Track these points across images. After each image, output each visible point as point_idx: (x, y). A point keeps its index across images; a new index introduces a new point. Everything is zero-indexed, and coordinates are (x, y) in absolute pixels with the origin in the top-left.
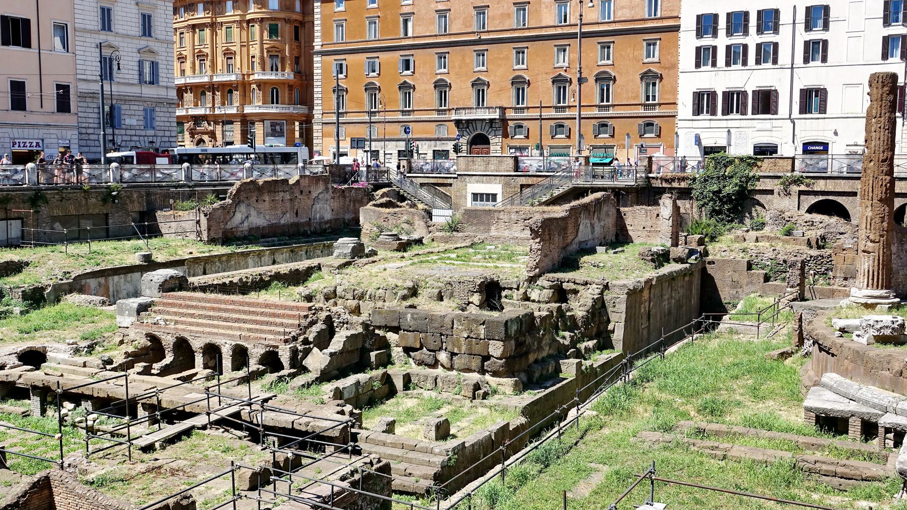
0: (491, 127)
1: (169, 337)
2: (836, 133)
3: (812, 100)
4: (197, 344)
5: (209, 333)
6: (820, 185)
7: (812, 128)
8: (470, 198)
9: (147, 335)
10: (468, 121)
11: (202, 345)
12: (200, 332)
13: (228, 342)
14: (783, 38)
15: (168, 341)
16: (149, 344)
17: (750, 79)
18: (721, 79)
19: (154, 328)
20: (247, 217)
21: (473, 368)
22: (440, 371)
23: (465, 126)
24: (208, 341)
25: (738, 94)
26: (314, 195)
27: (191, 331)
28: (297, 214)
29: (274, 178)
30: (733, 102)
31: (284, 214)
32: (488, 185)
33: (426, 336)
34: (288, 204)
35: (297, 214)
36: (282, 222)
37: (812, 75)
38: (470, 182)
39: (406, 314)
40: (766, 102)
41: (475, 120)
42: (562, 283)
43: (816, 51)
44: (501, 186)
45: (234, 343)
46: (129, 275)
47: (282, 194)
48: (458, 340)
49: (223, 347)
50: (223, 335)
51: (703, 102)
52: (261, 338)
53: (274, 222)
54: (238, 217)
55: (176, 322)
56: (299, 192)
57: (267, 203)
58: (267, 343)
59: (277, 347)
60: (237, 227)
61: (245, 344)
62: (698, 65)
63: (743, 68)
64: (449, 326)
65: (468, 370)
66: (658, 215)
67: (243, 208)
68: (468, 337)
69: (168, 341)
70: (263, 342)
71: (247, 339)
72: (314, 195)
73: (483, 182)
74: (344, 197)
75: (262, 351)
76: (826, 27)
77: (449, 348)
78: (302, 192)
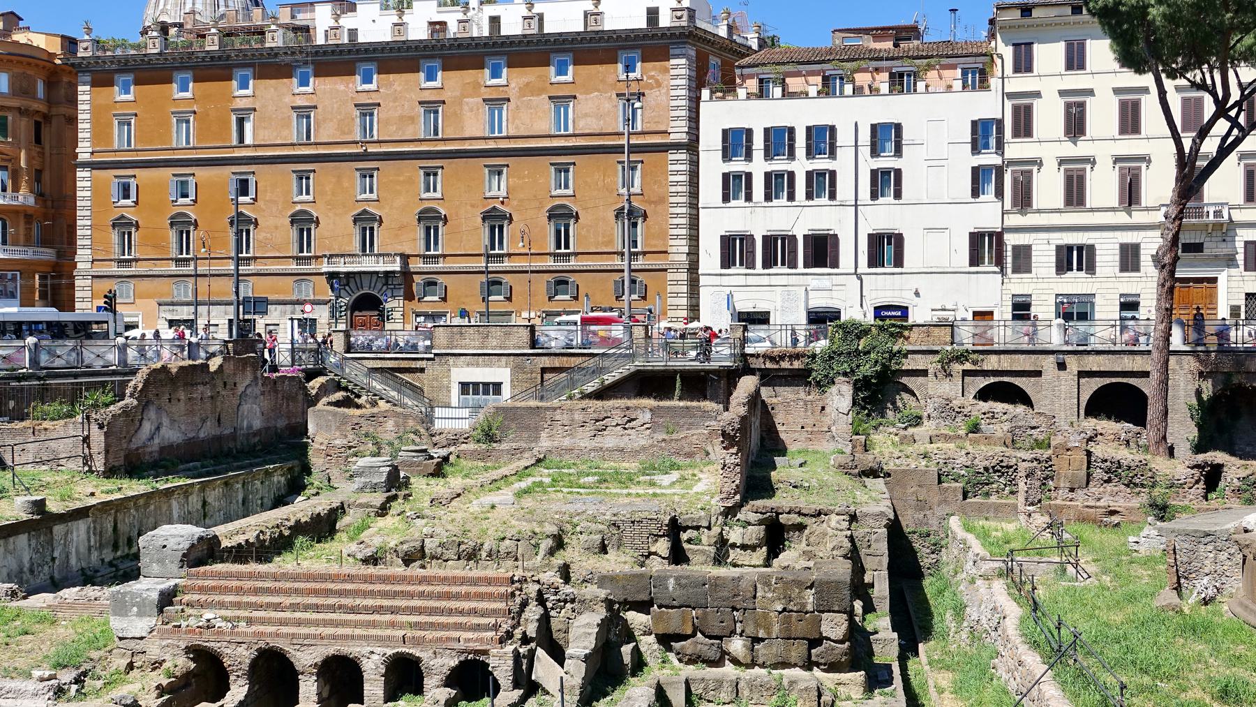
0: (386, 284)
1: (241, 650)
2: (917, 294)
3: (886, 249)
4: (305, 658)
5: (334, 637)
6: (992, 363)
7: (886, 287)
8: (455, 390)
9: (188, 650)
10: (348, 274)
11: (319, 660)
12: (315, 637)
13: (378, 650)
14: (842, 164)
15: (238, 657)
16: (193, 666)
18: (760, 219)
19: (207, 635)
20: (158, 428)
21: (793, 661)
22: (729, 669)
23: (344, 281)
24: (331, 651)
25: (783, 239)
26: (241, 389)
27: (293, 636)
28: (219, 420)
29: (191, 362)
30: (777, 250)
31: (204, 421)
32: (487, 370)
33: (705, 614)
34: (208, 405)
35: (219, 420)
36: (202, 435)
38: (456, 365)
39: (666, 578)
40: (822, 250)
41: (360, 273)
42: (778, 514)
43: (885, 183)
45: (390, 652)
46: (11, 540)
47: (201, 388)
48: (765, 616)
49: (365, 661)
50: (366, 638)
51: (734, 249)
52: (448, 639)
53: (191, 435)
54: (147, 427)
55: (250, 621)
56: (221, 384)
57: (182, 404)
58: (462, 645)
59: (485, 652)
60: (145, 446)
61: (416, 652)
62: (726, 198)
63: (747, 204)
64: (749, 595)
65: (785, 665)
66: (823, 408)
67: (152, 413)
68: (784, 610)
69: (238, 657)
70: (456, 646)
71: (418, 642)
72: (241, 389)
73: (478, 365)
74: (276, 392)
75: (454, 662)
76: (898, 152)
77: (750, 630)
78: (225, 384)
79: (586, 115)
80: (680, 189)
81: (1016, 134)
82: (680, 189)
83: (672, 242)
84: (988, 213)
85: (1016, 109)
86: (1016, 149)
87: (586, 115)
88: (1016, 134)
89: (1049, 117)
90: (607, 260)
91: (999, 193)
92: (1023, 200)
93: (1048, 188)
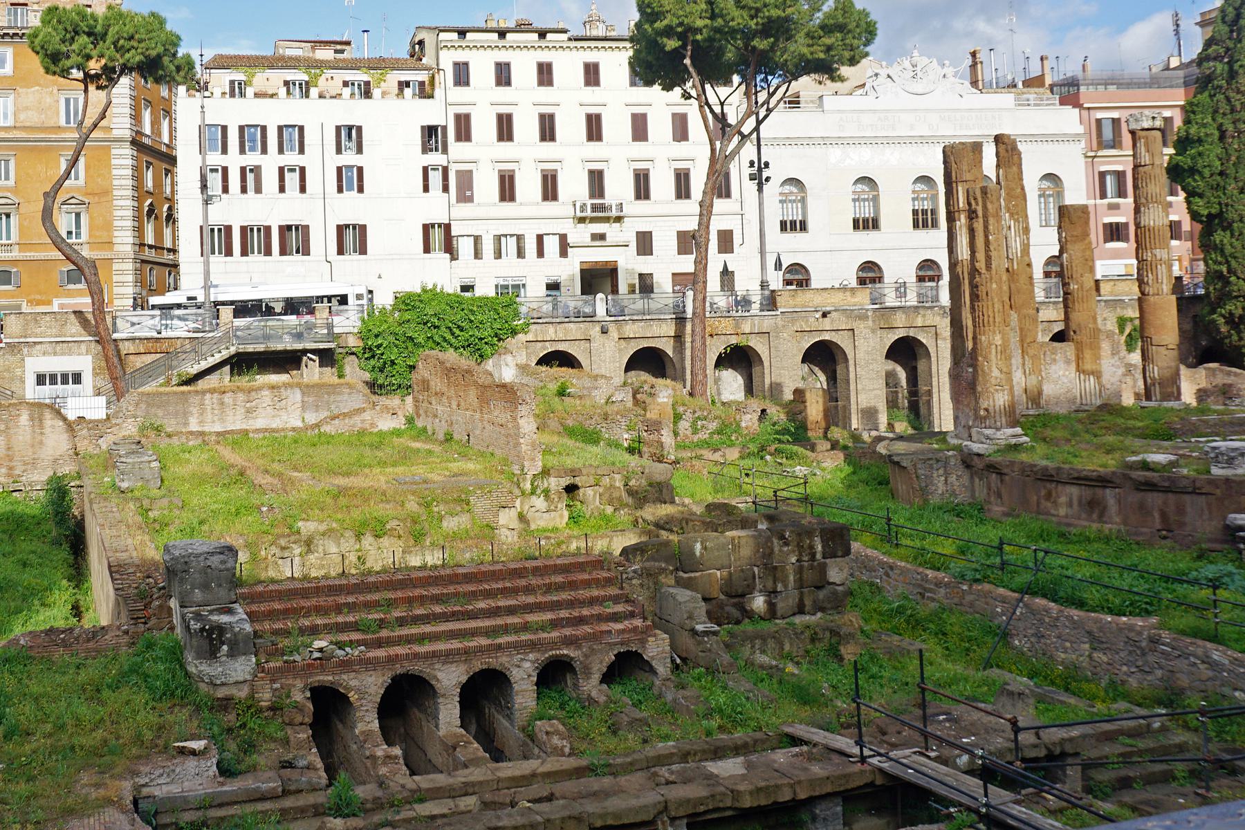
2: (380, 277)
3: (352, 238)
8: (31, 380)
14: (310, 160)
17: (270, 209)
18: (236, 210)
37: (349, 208)
38: (30, 355)
43: (350, 180)
44: (90, 357)
73: (55, 354)
76: (360, 150)
79: (27, 108)
80: (123, 182)
81: (459, 138)
82: (123, 182)
83: (116, 234)
84: (437, 207)
85: (458, 117)
86: (457, 150)
87: (27, 108)
88: (459, 138)
89: (484, 127)
90: (30, 251)
91: (446, 189)
92: (465, 196)
93: (485, 186)
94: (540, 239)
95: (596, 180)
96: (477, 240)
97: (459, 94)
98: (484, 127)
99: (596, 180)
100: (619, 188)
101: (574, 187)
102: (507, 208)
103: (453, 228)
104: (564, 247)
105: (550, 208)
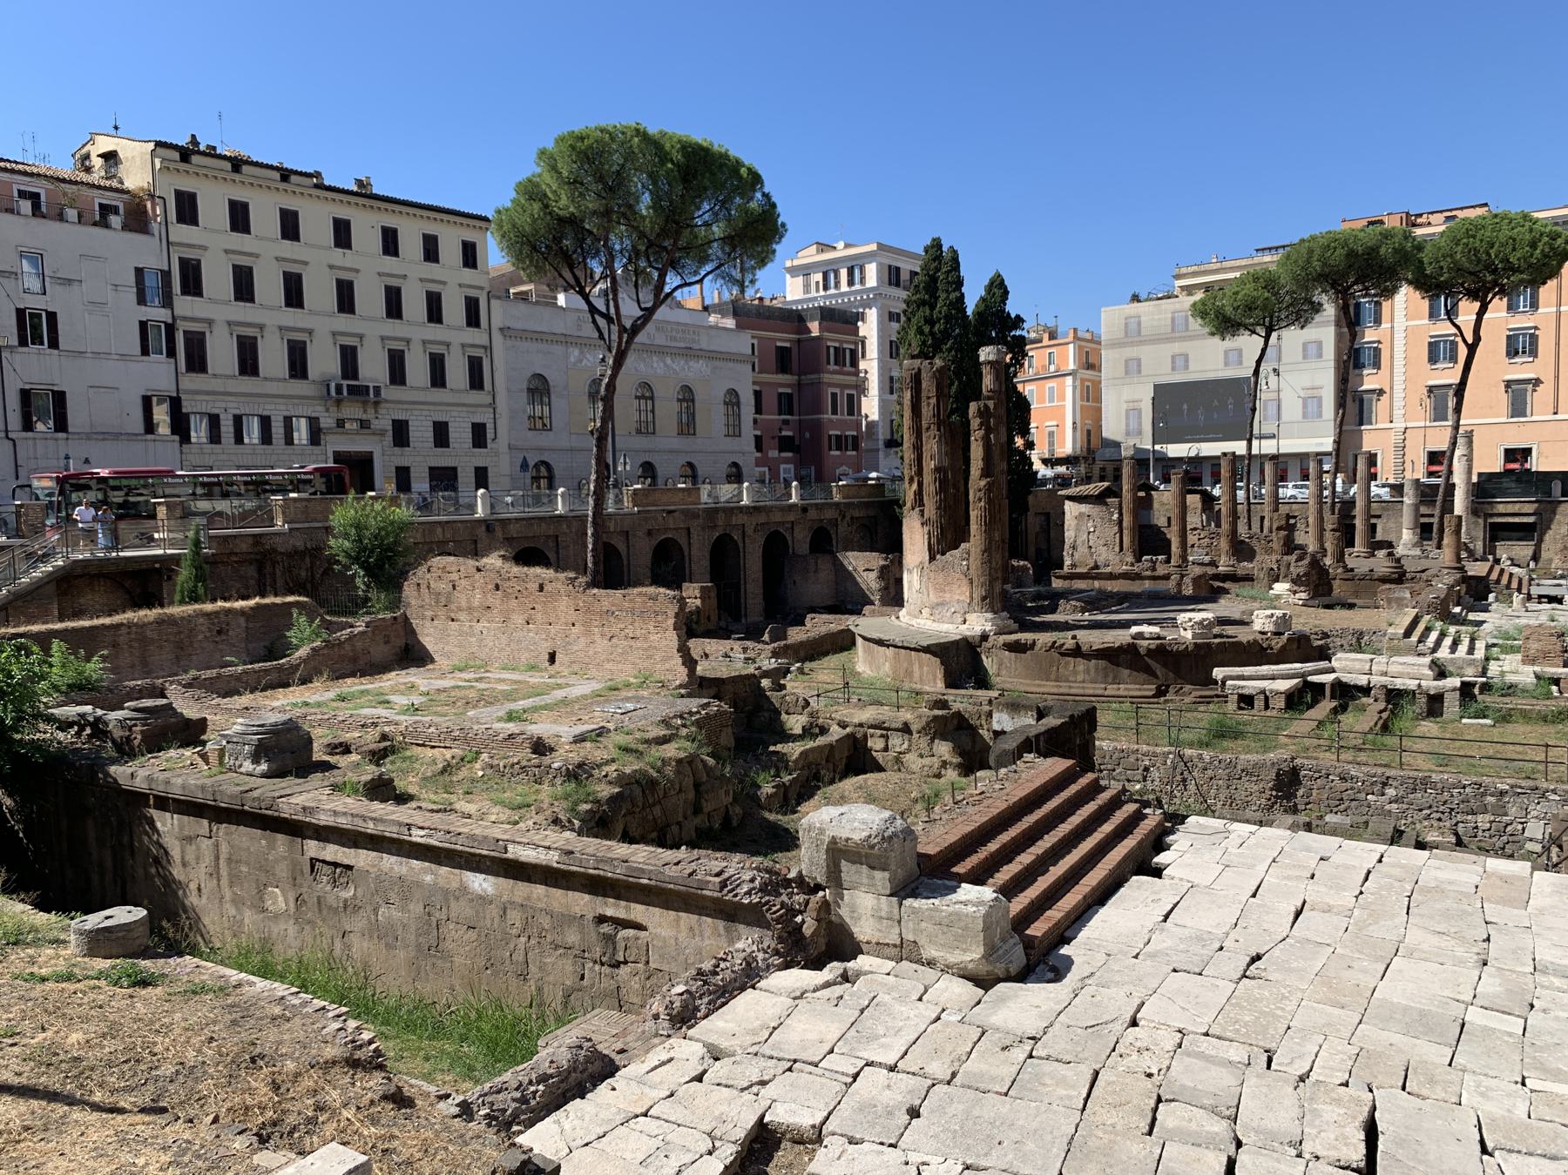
81: (185, 291)
84: (160, 373)
85: (184, 262)
86: (185, 305)
88: (185, 291)
89: (218, 280)
91: (172, 353)
92: (197, 362)
93: (223, 354)
94: (238, 421)
95: (349, 357)
96: (214, 421)
97: (182, 233)
98: (218, 280)
99: (349, 357)
100: (373, 368)
101: (324, 362)
102: (247, 384)
103: (184, 403)
104: (316, 435)
105: (298, 387)
